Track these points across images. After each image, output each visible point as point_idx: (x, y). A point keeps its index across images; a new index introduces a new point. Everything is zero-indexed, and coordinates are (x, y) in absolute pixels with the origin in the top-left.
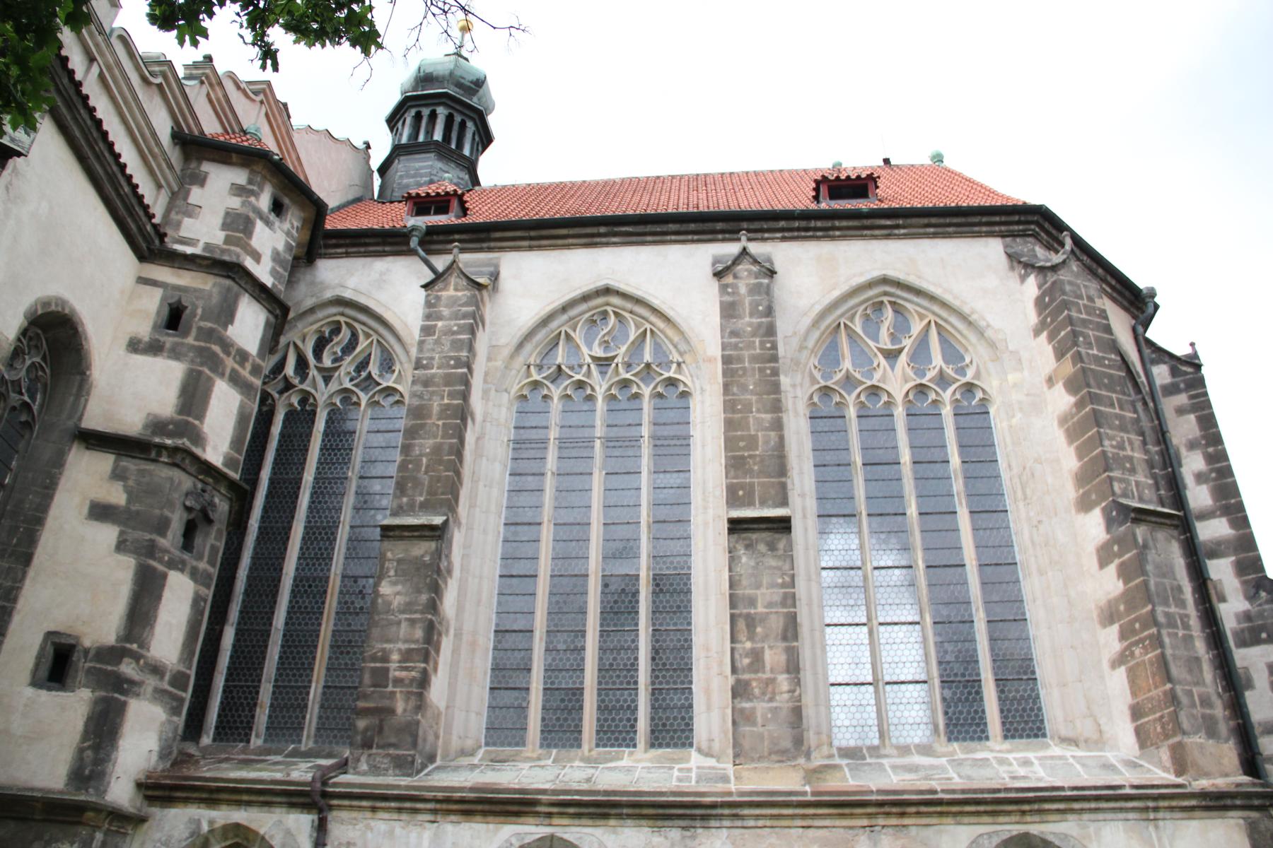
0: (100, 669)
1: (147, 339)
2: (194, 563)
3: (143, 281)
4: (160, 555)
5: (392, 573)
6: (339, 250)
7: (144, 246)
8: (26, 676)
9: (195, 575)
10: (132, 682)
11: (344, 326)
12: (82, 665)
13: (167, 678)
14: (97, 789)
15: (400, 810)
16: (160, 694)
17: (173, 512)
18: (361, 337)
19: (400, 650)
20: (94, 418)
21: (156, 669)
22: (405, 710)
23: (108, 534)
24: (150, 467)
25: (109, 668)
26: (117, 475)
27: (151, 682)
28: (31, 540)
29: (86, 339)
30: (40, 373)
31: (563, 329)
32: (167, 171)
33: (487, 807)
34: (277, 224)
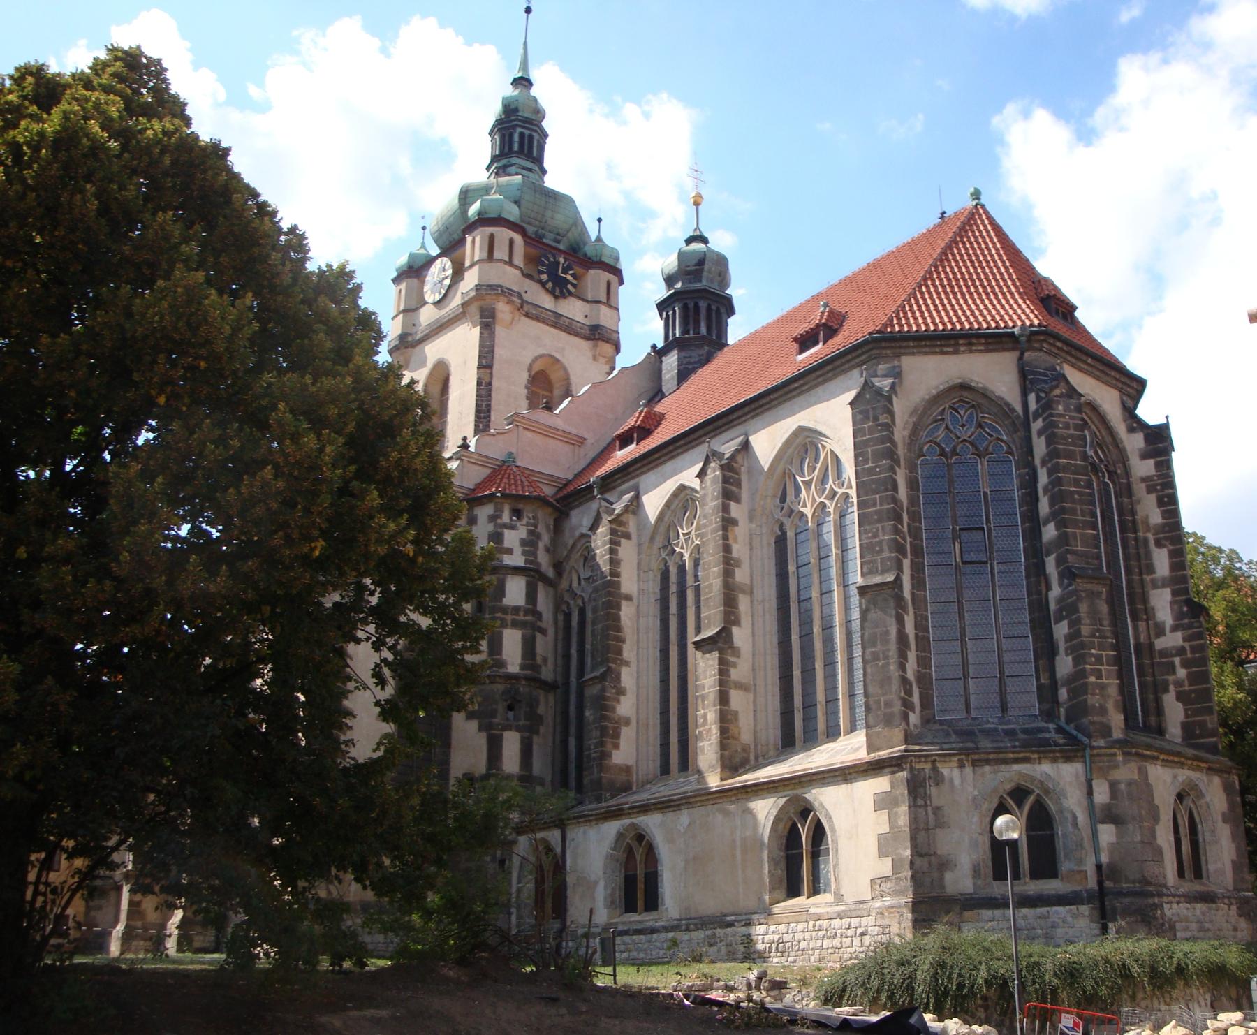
9: (518, 729)
34: (518, 524)
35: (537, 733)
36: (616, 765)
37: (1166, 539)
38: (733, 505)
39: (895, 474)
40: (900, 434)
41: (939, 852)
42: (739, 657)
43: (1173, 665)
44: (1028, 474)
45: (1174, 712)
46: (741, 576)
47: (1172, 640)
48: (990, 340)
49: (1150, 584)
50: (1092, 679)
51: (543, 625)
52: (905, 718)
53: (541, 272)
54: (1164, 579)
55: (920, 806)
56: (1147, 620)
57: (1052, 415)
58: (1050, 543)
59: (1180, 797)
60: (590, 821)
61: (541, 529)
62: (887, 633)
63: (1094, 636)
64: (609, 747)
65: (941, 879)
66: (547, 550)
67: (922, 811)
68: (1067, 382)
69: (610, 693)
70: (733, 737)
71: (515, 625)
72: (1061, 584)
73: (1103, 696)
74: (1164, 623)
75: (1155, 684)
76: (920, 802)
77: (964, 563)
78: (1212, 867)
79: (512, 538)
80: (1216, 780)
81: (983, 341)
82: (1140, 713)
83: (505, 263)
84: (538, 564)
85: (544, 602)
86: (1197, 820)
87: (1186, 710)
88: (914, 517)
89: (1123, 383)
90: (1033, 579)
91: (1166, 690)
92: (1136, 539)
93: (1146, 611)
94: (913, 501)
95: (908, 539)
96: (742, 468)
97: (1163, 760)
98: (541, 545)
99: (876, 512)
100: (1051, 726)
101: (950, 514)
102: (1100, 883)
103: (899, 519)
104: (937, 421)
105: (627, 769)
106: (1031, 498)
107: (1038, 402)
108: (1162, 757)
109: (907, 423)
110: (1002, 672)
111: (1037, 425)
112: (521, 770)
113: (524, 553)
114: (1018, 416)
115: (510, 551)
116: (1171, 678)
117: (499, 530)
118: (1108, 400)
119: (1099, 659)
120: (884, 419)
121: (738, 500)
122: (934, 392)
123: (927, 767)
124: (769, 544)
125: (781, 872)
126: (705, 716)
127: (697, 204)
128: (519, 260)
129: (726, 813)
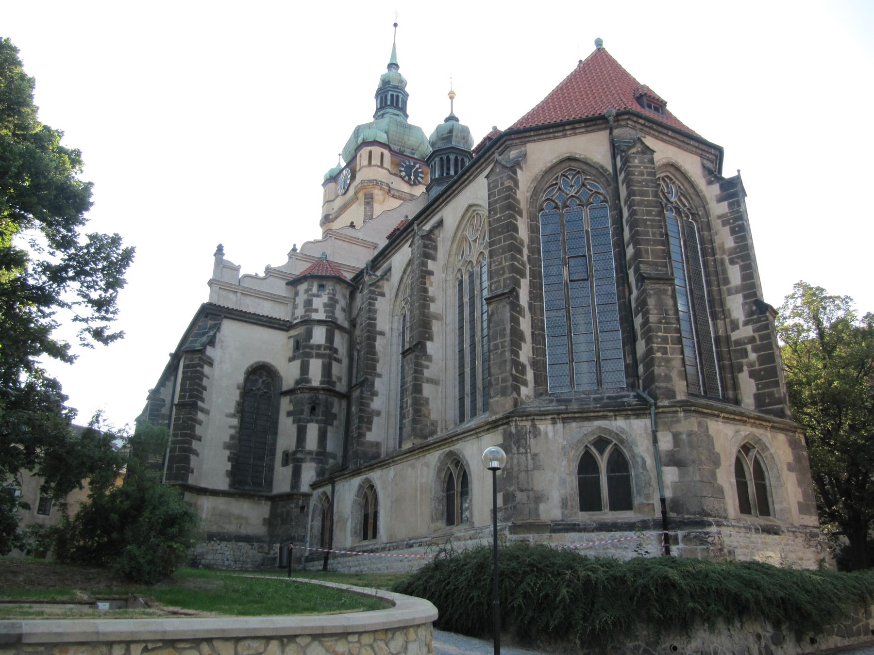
3: (290, 337)
9: (317, 422)
12: (290, 458)
13: (314, 454)
16: (312, 460)
20: (285, 388)
21: (310, 453)
23: (291, 419)
27: (309, 457)
35: (332, 425)
36: (369, 442)
37: (738, 257)
38: (430, 262)
39: (516, 220)
40: (523, 194)
41: (535, 489)
42: (431, 361)
43: (746, 350)
44: (617, 214)
45: (748, 387)
46: (433, 308)
47: (745, 332)
48: (588, 124)
49: (726, 293)
50: (659, 355)
51: (339, 356)
52: (517, 390)
53: (401, 171)
54: (737, 287)
55: (522, 453)
56: (725, 319)
57: (629, 167)
58: (630, 259)
59: (746, 448)
60: (346, 478)
61: (338, 296)
62: (505, 329)
63: (660, 322)
64: (364, 429)
65: (537, 509)
66: (343, 310)
67: (523, 457)
68: (643, 143)
69: (367, 394)
70: (424, 416)
71: (318, 356)
72: (637, 288)
73: (668, 367)
74: (738, 320)
75: (731, 365)
76: (522, 450)
77: (571, 281)
78: (777, 507)
79: (319, 303)
80: (781, 437)
81: (583, 125)
82: (720, 389)
83: (378, 166)
84: (336, 319)
85: (340, 342)
86: (764, 469)
87: (757, 385)
88: (534, 251)
89: (702, 150)
90: (620, 288)
91: (741, 370)
92: (715, 261)
93: (723, 312)
94: (534, 240)
95: (528, 266)
96: (439, 239)
97: (724, 418)
98: (338, 307)
99: (501, 247)
100: (632, 394)
101: (561, 248)
102: (664, 513)
103: (520, 252)
104: (553, 185)
105: (377, 445)
106: (619, 231)
107: (621, 161)
108: (722, 415)
109: (529, 187)
110: (598, 358)
111: (621, 178)
113: (325, 311)
114: (609, 174)
115: (316, 311)
116: (744, 361)
117: (310, 298)
118: (691, 164)
119: (665, 340)
120: (508, 183)
121: (434, 259)
122: (549, 165)
123: (528, 424)
124: (454, 286)
125: (442, 508)
126: (407, 401)
127: (452, 98)
128: (387, 163)
129: (413, 467)
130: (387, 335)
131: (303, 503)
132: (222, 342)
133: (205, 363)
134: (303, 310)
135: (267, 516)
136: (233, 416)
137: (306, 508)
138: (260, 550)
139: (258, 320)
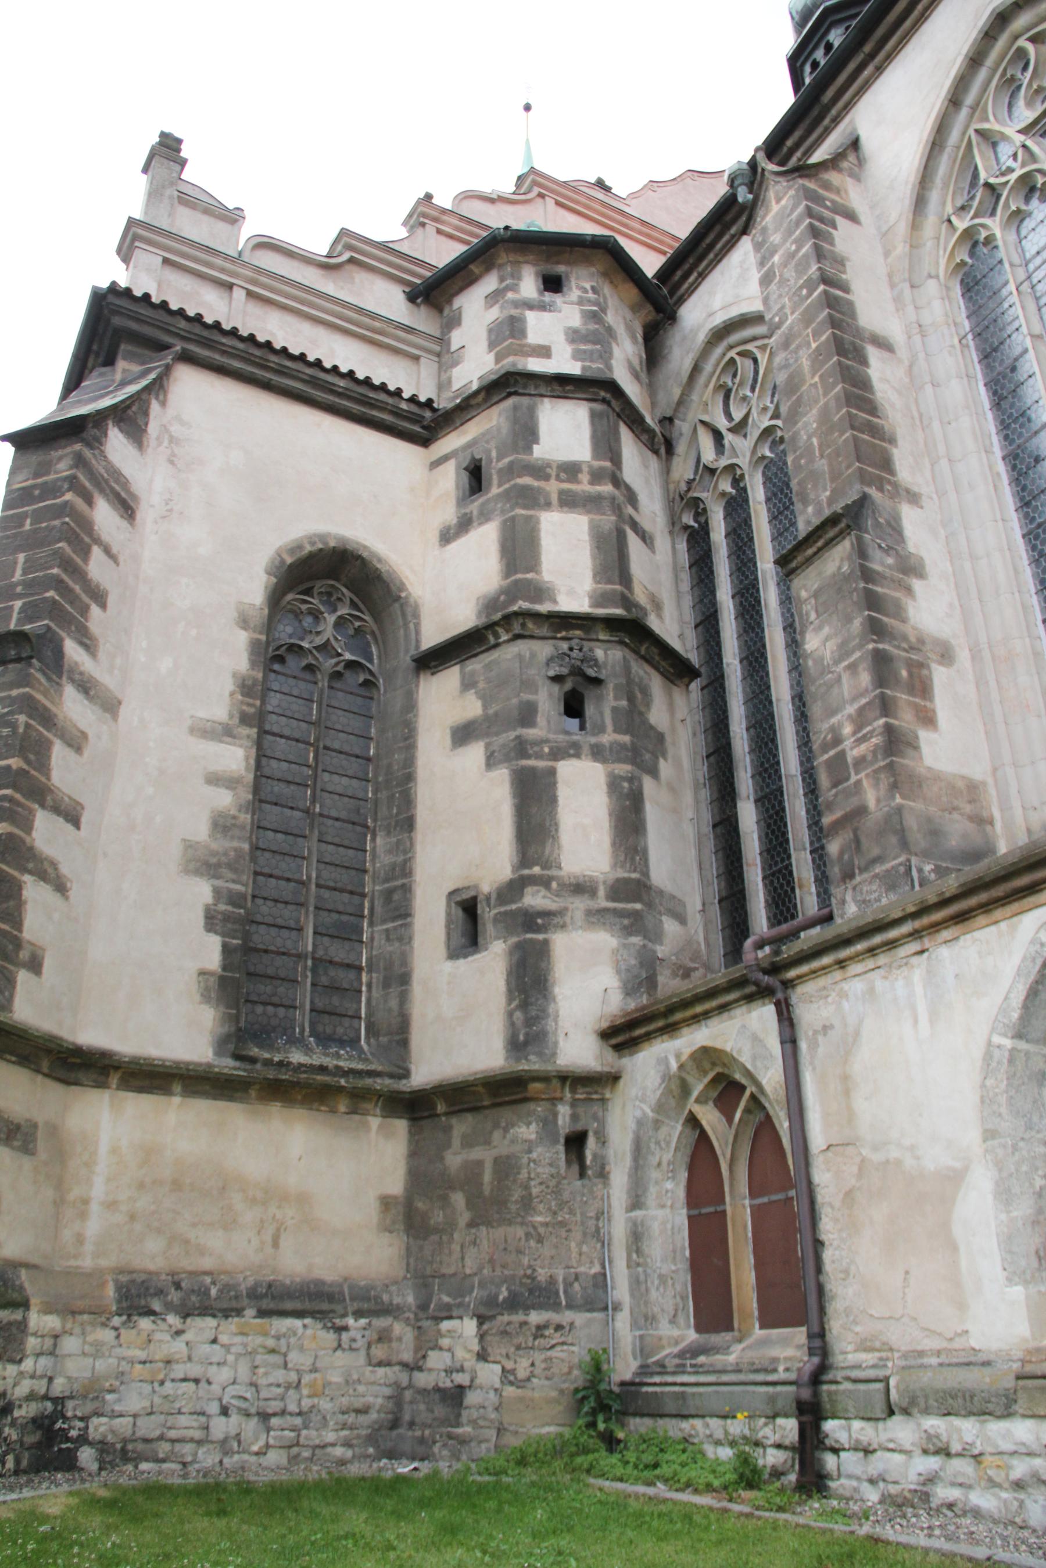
0: (506, 913)
1: (455, 521)
2: (593, 740)
3: (435, 464)
4: (536, 749)
5: (813, 616)
6: (691, 279)
7: (417, 428)
8: (442, 950)
9: (598, 753)
10: (547, 914)
11: (738, 358)
12: (487, 914)
13: (601, 892)
14: (540, 1054)
15: (872, 951)
16: (596, 917)
17: (536, 692)
18: (759, 356)
19: (850, 716)
21: (581, 888)
22: (878, 801)
23: (475, 753)
24: (494, 655)
25: (514, 907)
26: (467, 684)
27: (578, 905)
28: (408, 801)
29: (380, 560)
30: (357, 624)
31: (971, 132)
32: (410, 337)
33: (983, 897)
35: (653, 772)
71: (569, 502)
112: (614, 866)
115: (544, 352)
117: (514, 312)
130: (902, 352)
131: (574, 1117)
132: (172, 440)
133: (102, 491)
134: (490, 358)
135: (395, 1185)
136: (225, 733)
137: (591, 1143)
138: (379, 1352)
139: (314, 382)
